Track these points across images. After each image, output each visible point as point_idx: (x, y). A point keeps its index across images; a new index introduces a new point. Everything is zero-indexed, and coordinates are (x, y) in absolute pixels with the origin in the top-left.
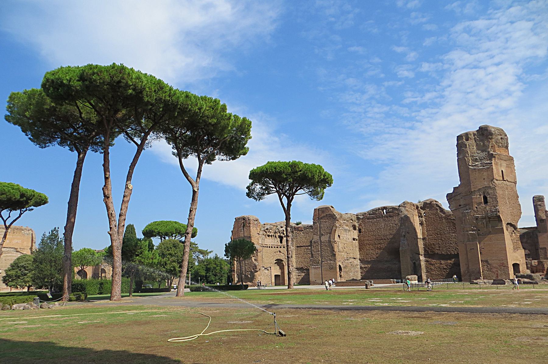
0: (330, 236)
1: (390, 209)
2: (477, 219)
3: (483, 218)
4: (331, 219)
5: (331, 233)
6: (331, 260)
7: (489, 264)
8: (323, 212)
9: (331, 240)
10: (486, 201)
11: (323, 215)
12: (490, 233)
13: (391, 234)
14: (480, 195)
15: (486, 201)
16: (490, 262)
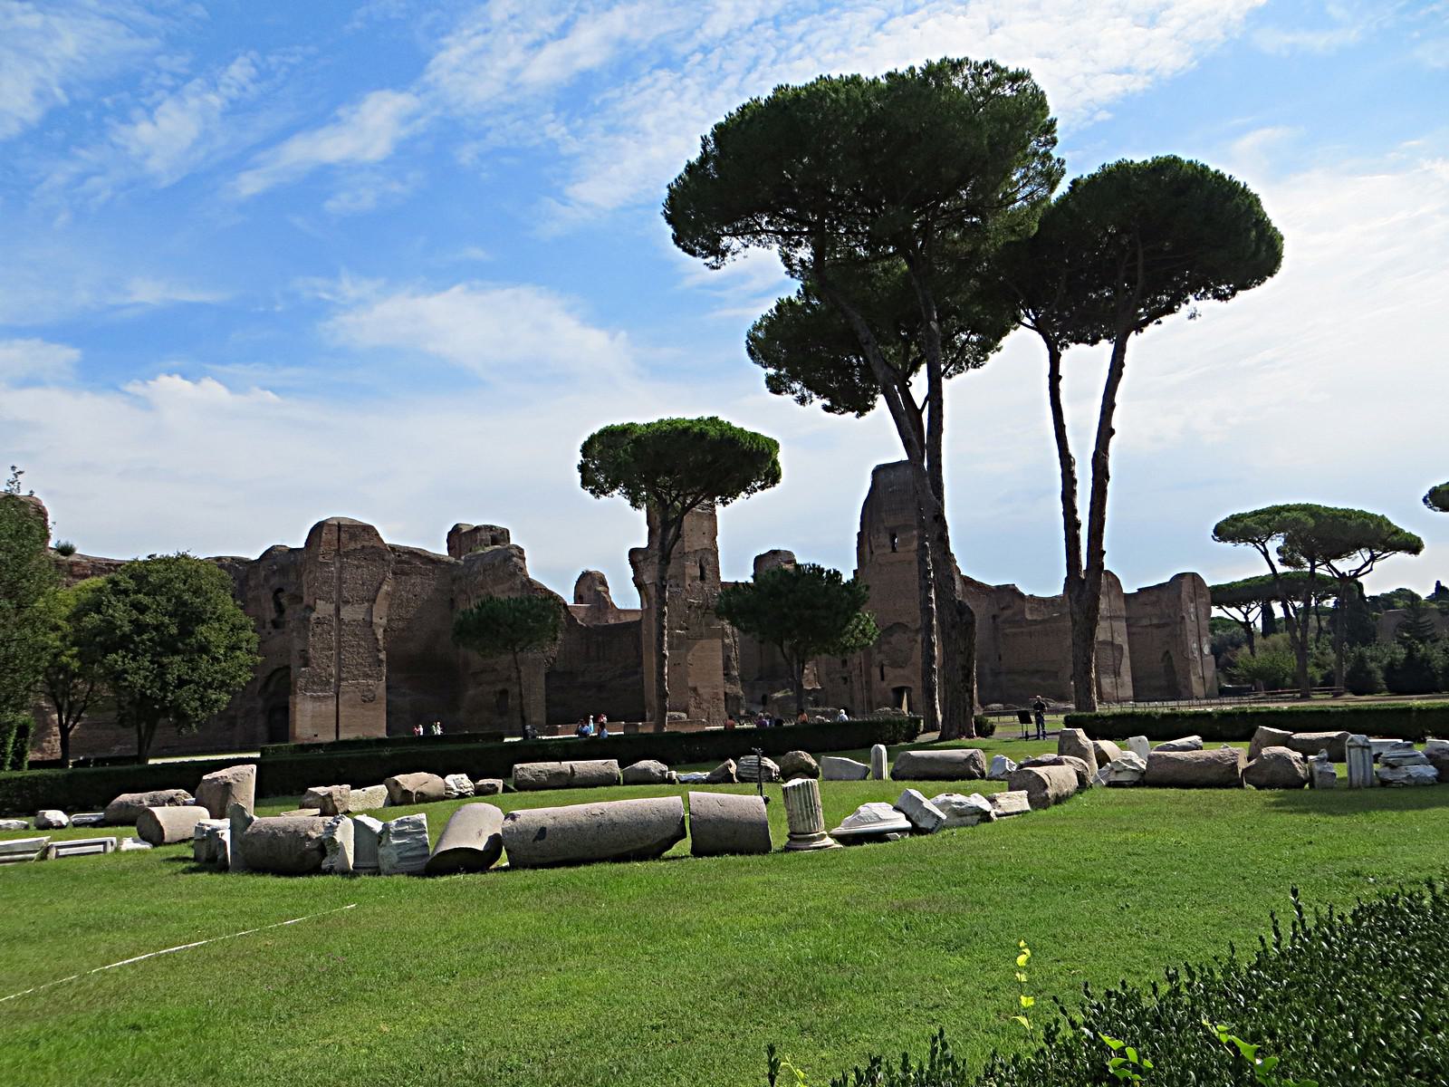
0: (370, 611)
1: (404, 553)
2: (690, 607)
3: (699, 607)
4: (375, 560)
5: (374, 601)
6: (367, 676)
7: (698, 694)
8: (353, 537)
9: (375, 620)
10: (702, 578)
11: (352, 546)
12: (701, 637)
13: (401, 619)
14: (696, 562)
15: (702, 578)
16: (701, 691)
